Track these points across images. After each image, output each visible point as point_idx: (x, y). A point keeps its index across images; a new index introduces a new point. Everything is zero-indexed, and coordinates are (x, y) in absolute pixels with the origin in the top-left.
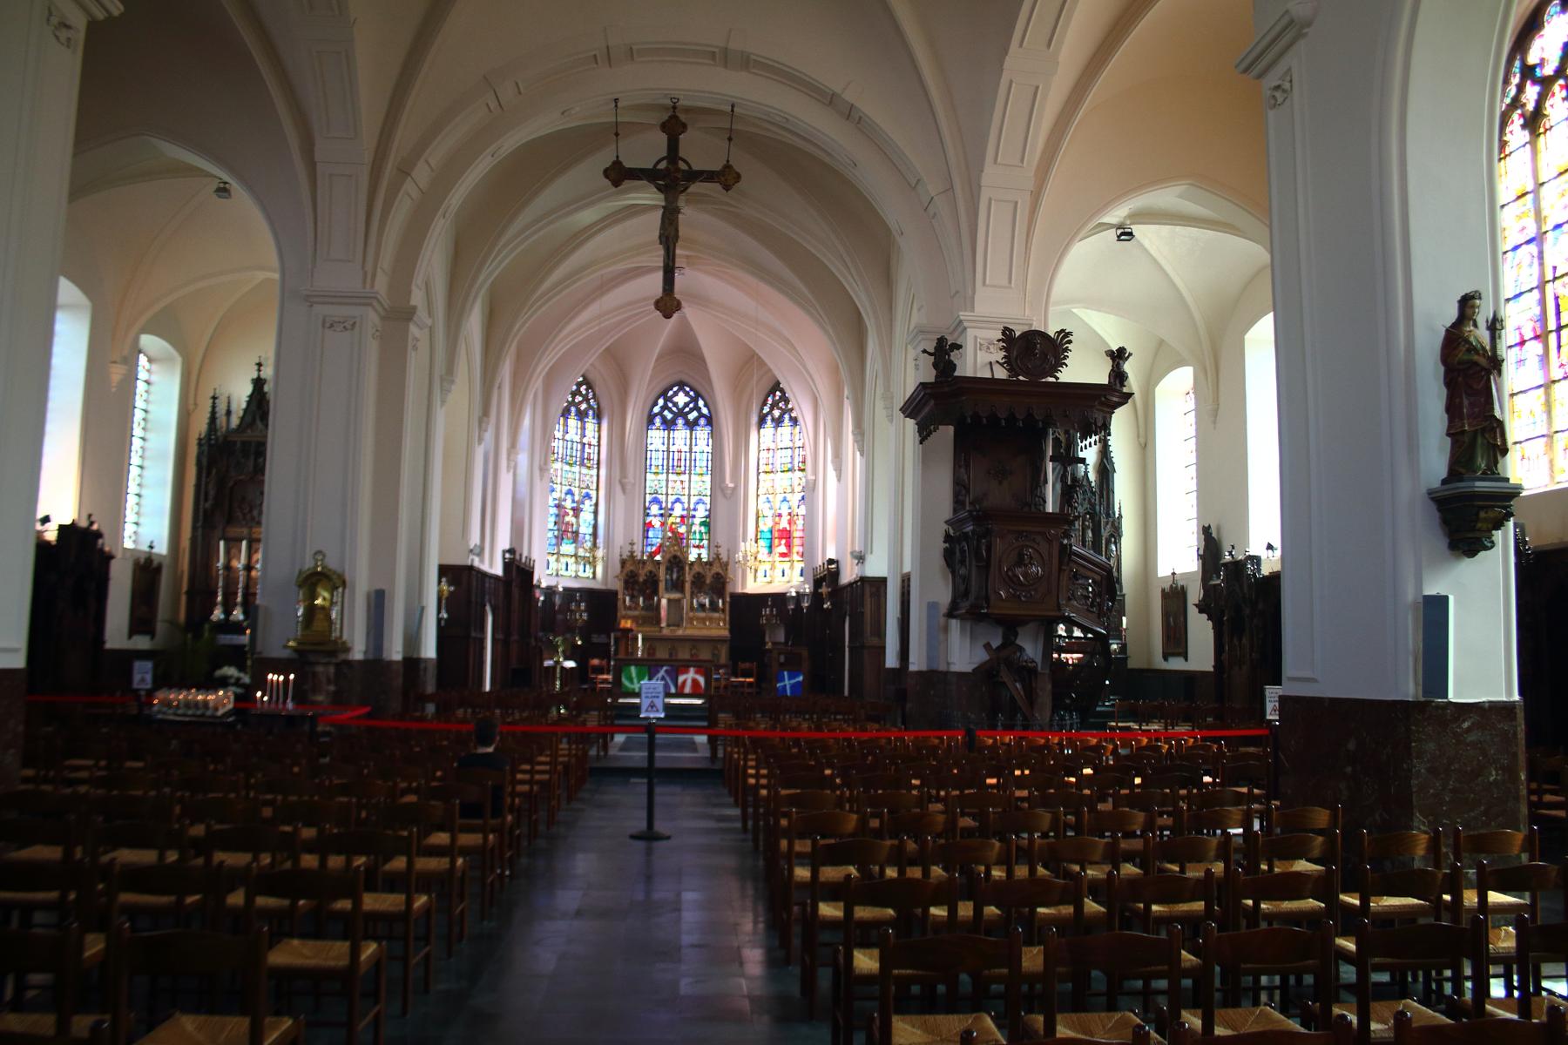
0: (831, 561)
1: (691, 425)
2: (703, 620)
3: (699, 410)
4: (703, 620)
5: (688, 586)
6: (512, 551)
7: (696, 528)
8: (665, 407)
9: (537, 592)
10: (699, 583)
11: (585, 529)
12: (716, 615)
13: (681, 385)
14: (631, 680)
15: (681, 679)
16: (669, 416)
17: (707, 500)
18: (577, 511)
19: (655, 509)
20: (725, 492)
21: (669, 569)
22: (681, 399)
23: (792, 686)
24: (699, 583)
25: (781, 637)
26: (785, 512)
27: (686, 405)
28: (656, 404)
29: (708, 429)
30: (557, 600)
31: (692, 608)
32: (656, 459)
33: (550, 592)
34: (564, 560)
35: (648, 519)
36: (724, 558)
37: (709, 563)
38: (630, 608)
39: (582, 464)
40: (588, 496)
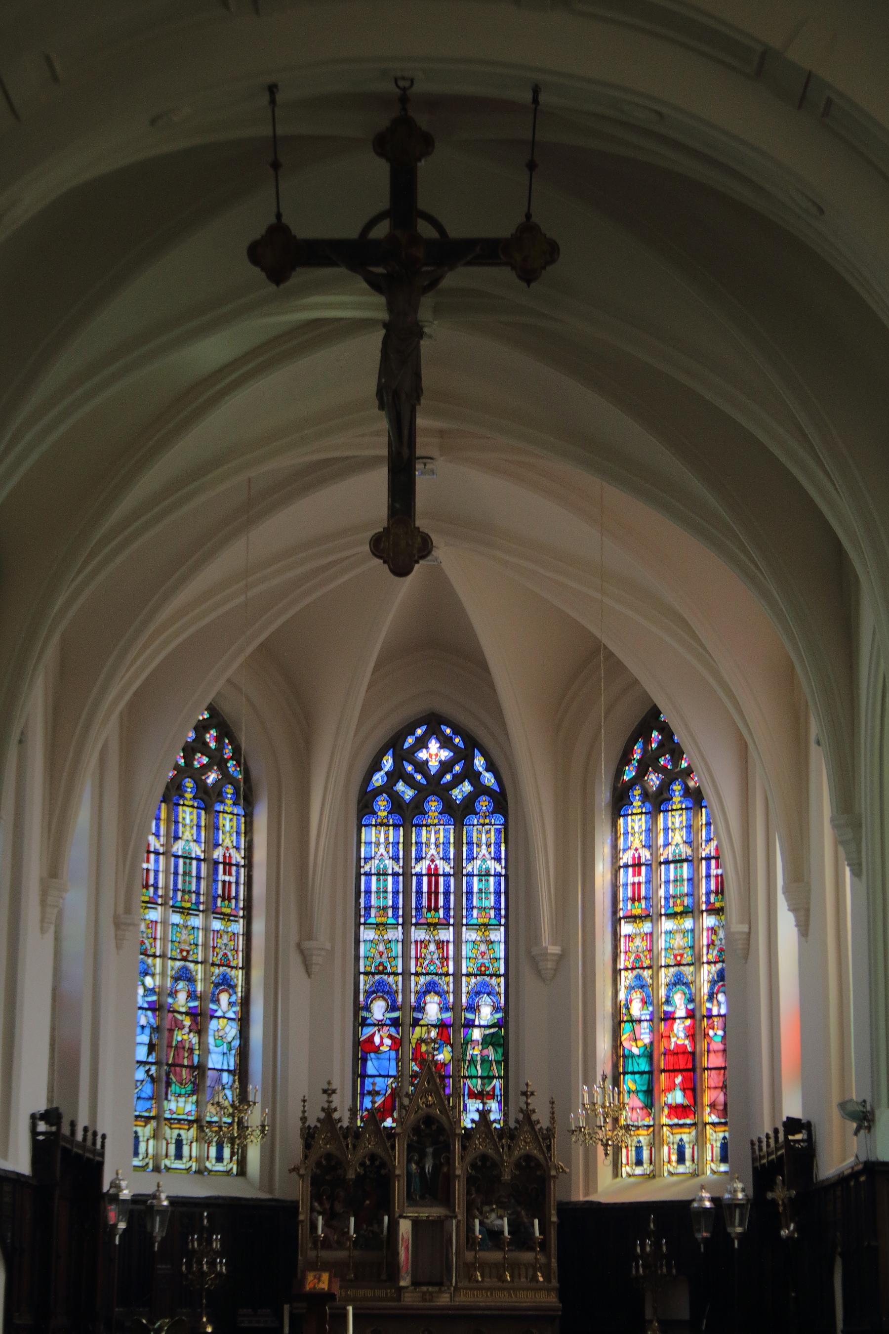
0: (793, 1125)
1: (458, 814)
2: (496, 1270)
4: (496, 1270)
5: (459, 1188)
6: (51, 1116)
9: (112, 1213)
10: (485, 1181)
11: (218, 1059)
12: (528, 1256)
13: (434, 723)
16: (408, 793)
18: (200, 1019)
19: (379, 1009)
20: (543, 964)
21: (415, 1150)
22: (434, 754)
24: (485, 1181)
27: (446, 766)
28: (376, 766)
30: (158, 1229)
31: (470, 1241)
32: (382, 892)
33: (141, 1207)
34: (172, 1134)
36: (542, 1118)
37: (508, 1134)
38: (326, 1244)
39: (213, 911)
40: (226, 984)
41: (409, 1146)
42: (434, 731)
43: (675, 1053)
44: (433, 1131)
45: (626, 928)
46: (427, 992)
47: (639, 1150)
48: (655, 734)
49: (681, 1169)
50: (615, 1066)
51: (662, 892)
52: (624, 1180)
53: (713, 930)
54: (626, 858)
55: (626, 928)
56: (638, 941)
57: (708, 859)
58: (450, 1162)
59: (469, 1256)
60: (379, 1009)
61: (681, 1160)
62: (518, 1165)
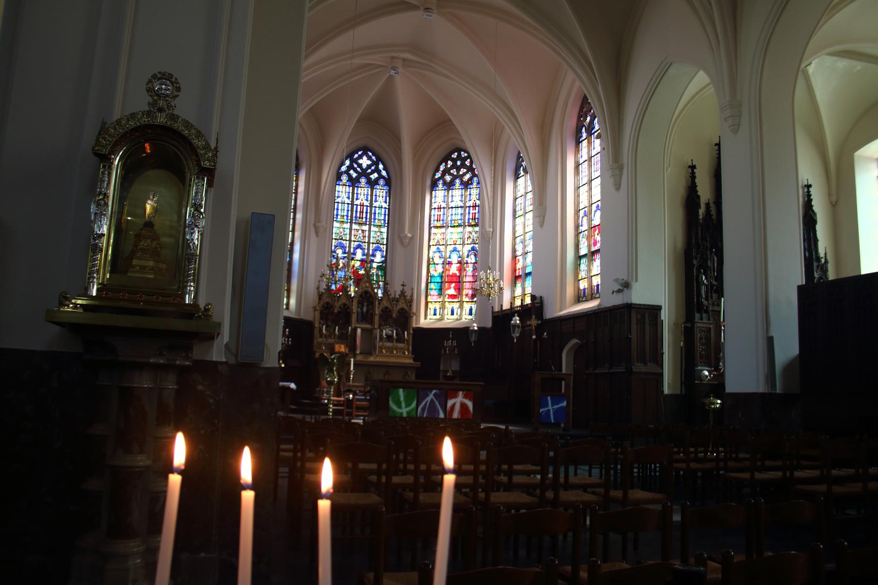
1: (372, 184)
2: (390, 350)
3: (379, 172)
4: (390, 350)
5: (377, 319)
8: (350, 167)
12: (401, 345)
13: (365, 150)
14: (399, 405)
15: (450, 403)
16: (354, 175)
17: (384, 248)
21: (360, 303)
22: (365, 162)
23: (556, 412)
26: (455, 259)
27: (369, 167)
28: (342, 164)
29: (386, 188)
32: (342, 210)
36: (408, 294)
41: (359, 303)
42: (365, 153)
43: (451, 276)
44: (367, 297)
45: (433, 230)
46: (357, 248)
47: (435, 310)
48: (449, 162)
49: (452, 317)
51: (449, 218)
52: (428, 320)
53: (470, 233)
54: (435, 206)
55: (433, 230)
56: (438, 235)
57: (469, 207)
58: (373, 309)
60: (340, 252)
61: (452, 314)
62: (398, 312)
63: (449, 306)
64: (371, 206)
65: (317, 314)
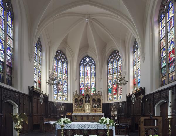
1: (90, 66)
3: (91, 62)
7: (92, 89)
8: (84, 62)
12: (99, 108)
13: (87, 56)
16: (85, 64)
19: (82, 85)
22: (88, 60)
25: (116, 113)
27: (89, 61)
28: (81, 61)
29: (94, 66)
32: (82, 74)
35: (81, 88)
36: (100, 94)
40: (65, 82)
41: (86, 97)
42: (88, 57)
44: (88, 96)
45: (109, 76)
47: (110, 98)
50: (107, 90)
55: (109, 76)
59: (92, 108)
63: (114, 97)
64: (90, 72)
65: (74, 101)
